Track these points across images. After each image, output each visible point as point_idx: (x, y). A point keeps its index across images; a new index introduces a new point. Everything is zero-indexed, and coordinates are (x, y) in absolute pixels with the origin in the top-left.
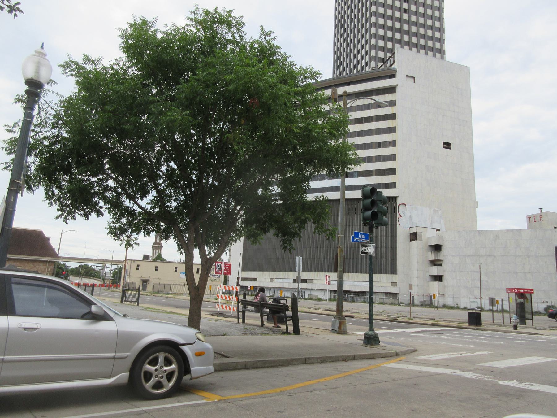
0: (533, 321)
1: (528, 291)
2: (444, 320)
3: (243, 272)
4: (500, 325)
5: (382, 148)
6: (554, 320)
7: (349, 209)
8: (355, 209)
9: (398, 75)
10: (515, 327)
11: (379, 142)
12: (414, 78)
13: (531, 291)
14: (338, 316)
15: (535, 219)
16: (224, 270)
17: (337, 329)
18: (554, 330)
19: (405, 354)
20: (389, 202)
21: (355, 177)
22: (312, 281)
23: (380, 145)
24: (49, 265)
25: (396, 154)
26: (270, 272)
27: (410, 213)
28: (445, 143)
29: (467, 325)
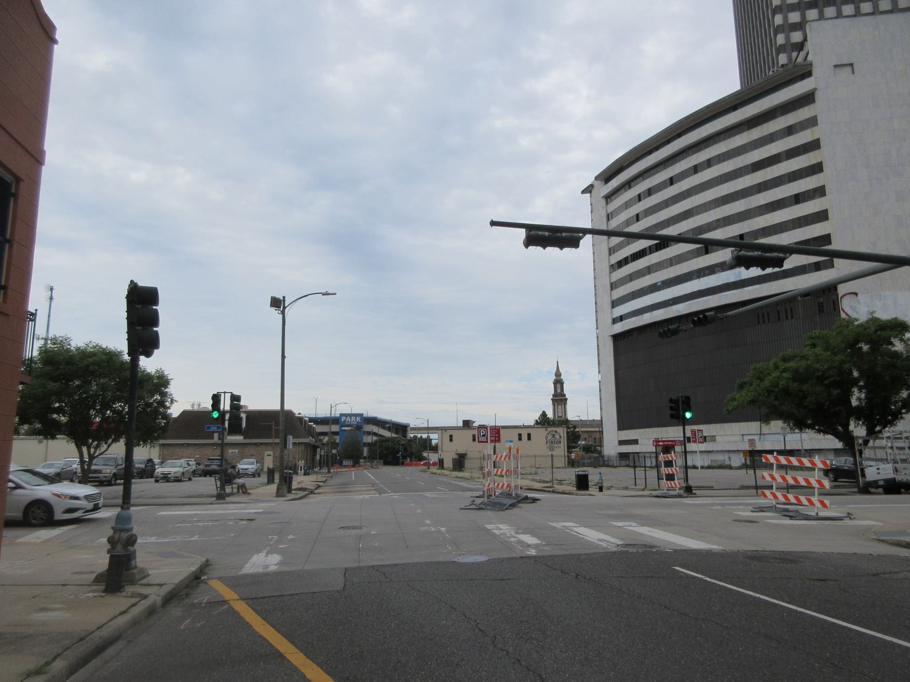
3: (620, 432)
5: (803, 202)
7: (758, 315)
8: (768, 314)
12: (851, 65)
16: (491, 437)
22: (713, 439)
24: (299, 447)
27: (868, 306)
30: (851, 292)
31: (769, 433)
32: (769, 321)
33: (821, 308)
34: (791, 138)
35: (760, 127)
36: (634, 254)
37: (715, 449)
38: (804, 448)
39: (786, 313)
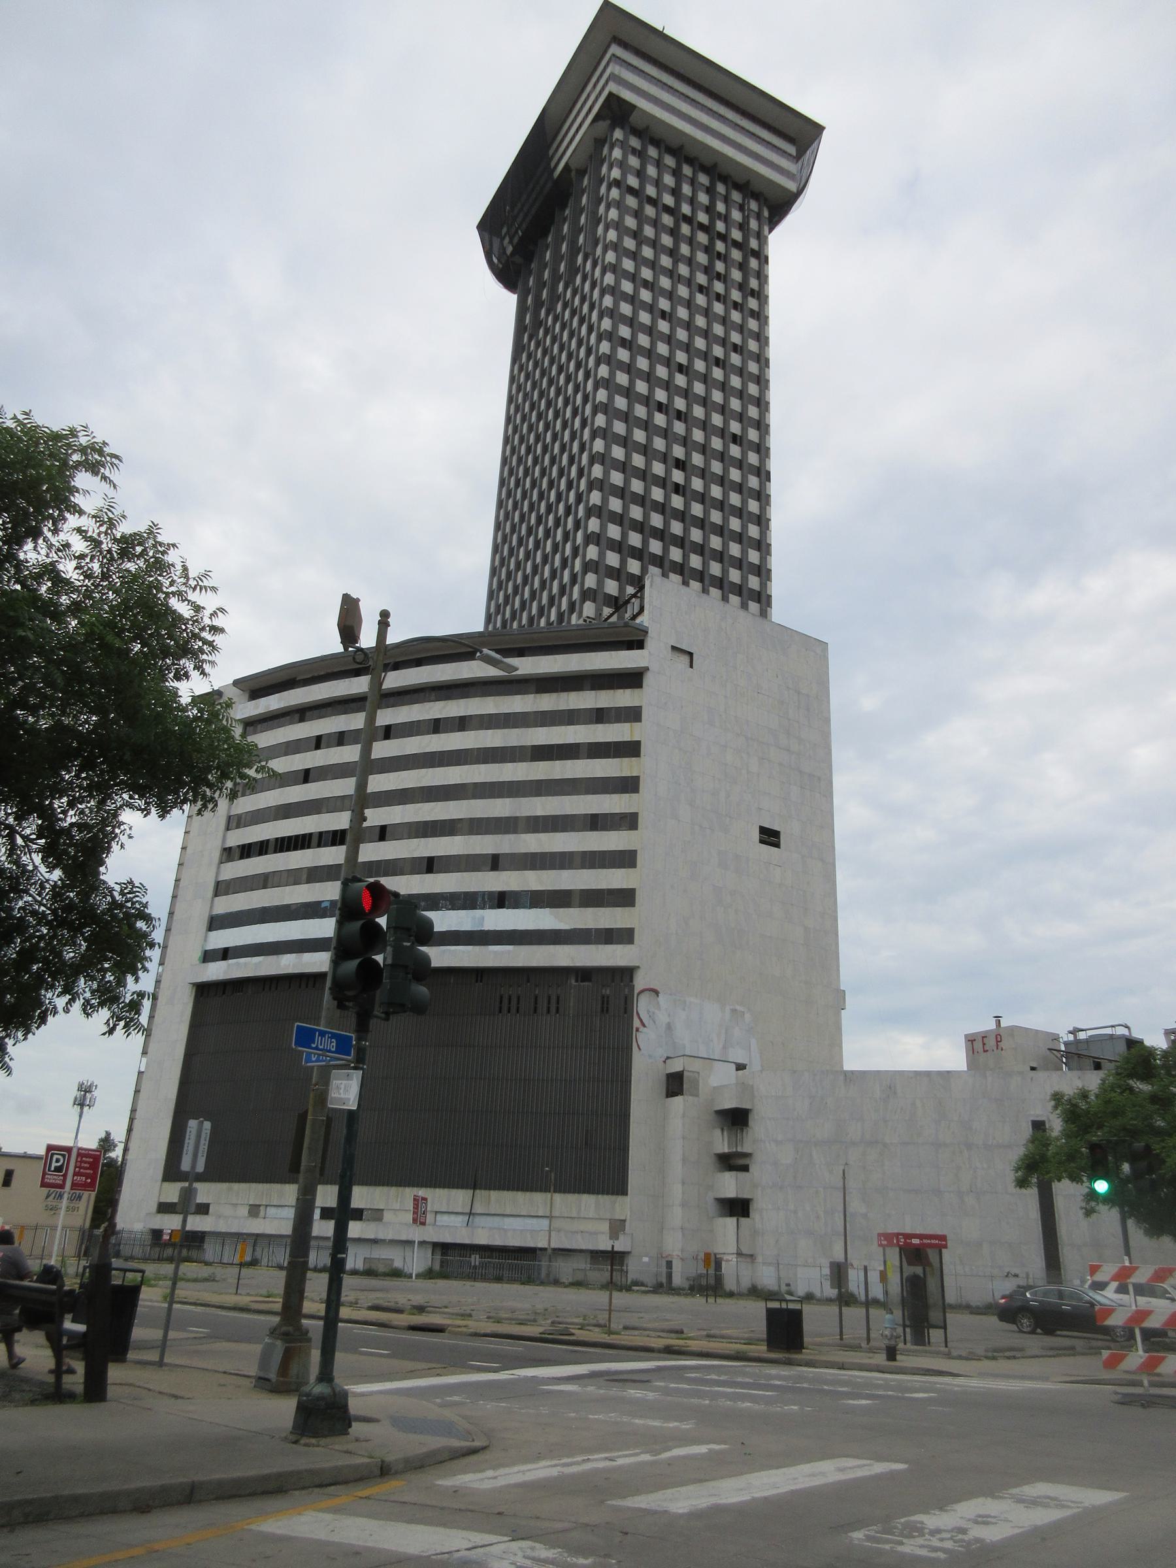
0: (948, 1331)
1: (933, 1241)
2: (708, 1336)
3: (166, 1184)
4: (856, 1348)
6: (1014, 1327)
8: (519, 998)
9: (650, 643)
10: (892, 1353)
11: (592, 815)
12: (691, 654)
13: (940, 1242)
14: (284, 1329)
15: (984, 1044)
16: (75, 1174)
17: (273, 1376)
18: (994, 1358)
19: (422, 1467)
20: (613, 981)
21: (524, 907)
22: (377, 1215)
23: (596, 822)
25: (636, 851)
26: (254, 1185)
27: (669, 1015)
28: (763, 831)
29: (762, 1349)
30: (652, 987)
31: (487, 1212)
32: (518, 1011)
33: (605, 1005)
34: (435, 737)
35: (554, 695)
36: (283, 839)
37: (381, 1236)
38: (553, 1245)
39: (549, 1002)
